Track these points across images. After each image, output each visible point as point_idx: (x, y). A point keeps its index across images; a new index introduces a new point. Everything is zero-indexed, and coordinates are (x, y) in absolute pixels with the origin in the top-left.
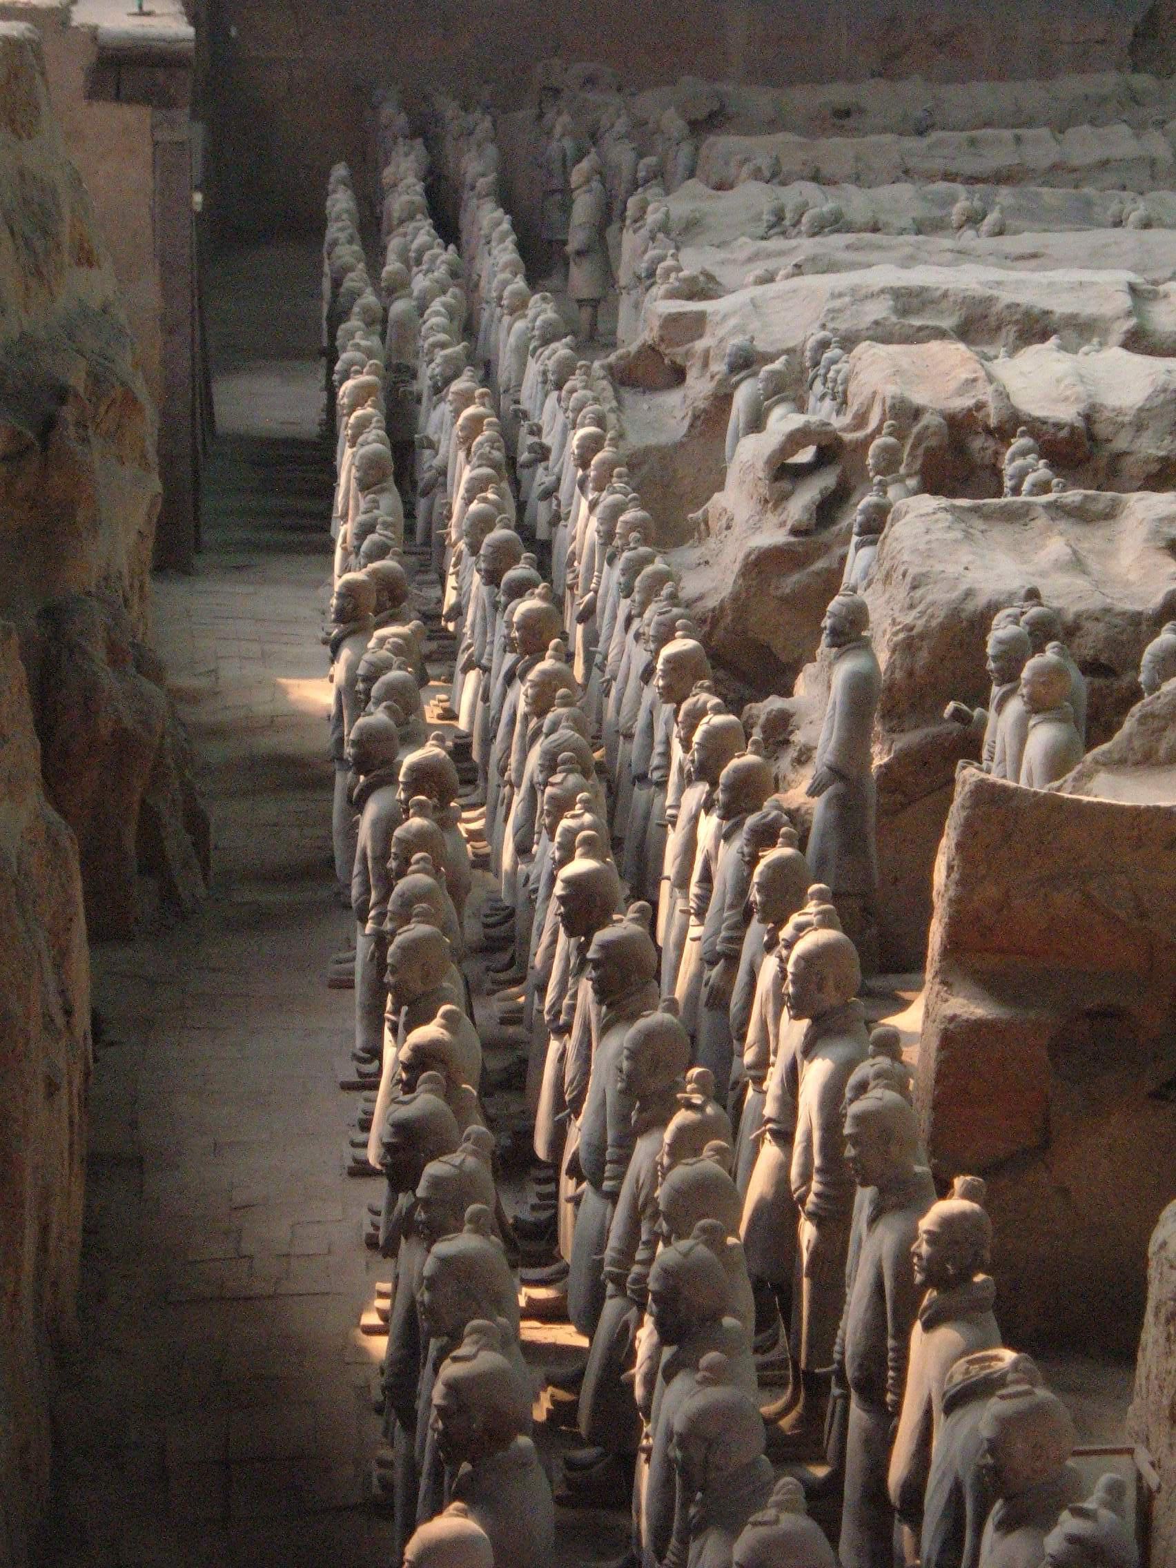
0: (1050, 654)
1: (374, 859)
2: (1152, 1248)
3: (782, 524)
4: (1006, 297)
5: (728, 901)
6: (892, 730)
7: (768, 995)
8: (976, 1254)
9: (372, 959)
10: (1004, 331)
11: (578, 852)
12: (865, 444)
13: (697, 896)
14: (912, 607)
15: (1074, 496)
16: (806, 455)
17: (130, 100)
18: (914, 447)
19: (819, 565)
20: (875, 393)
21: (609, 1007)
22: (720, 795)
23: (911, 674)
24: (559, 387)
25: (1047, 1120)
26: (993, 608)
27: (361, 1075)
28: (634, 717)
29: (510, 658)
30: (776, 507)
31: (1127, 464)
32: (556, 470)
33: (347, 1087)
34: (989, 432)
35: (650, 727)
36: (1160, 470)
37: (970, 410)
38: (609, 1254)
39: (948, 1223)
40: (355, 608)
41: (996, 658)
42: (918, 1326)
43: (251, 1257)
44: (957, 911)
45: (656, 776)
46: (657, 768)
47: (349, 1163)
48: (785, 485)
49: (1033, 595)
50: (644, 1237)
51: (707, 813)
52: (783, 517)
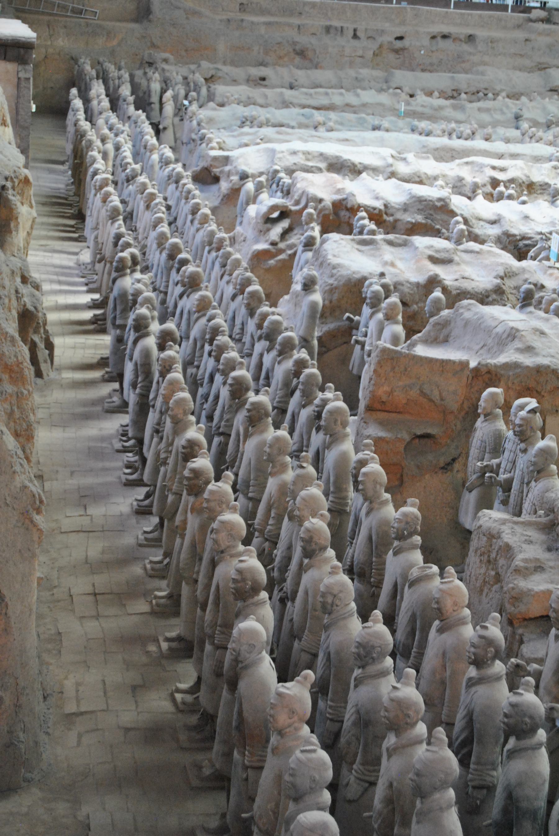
0: (394, 299)
1: (141, 365)
3: (266, 241)
5: (279, 386)
6: (322, 323)
9: (138, 403)
11: (237, 367)
14: (332, 276)
15: (391, 237)
16: (275, 215)
17: (10, 61)
19: (282, 257)
20: (303, 192)
23: (331, 302)
24: (177, 182)
25: (402, 476)
26: (365, 279)
27: (123, 446)
29: (179, 289)
30: (265, 234)
31: (399, 226)
32: (175, 215)
33: (118, 451)
34: (347, 209)
35: (234, 318)
36: (412, 228)
38: (257, 521)
39: (405, 515)
41: (370, 298)
42: (391, 552)
43: (91, 516)
44: (373, 396)
45: (237, 337)
46: (238, 334)
47: (124, 481)
48: (269, 225)
49: (382, 275)
50: (273, 515)
51: (268, 353)
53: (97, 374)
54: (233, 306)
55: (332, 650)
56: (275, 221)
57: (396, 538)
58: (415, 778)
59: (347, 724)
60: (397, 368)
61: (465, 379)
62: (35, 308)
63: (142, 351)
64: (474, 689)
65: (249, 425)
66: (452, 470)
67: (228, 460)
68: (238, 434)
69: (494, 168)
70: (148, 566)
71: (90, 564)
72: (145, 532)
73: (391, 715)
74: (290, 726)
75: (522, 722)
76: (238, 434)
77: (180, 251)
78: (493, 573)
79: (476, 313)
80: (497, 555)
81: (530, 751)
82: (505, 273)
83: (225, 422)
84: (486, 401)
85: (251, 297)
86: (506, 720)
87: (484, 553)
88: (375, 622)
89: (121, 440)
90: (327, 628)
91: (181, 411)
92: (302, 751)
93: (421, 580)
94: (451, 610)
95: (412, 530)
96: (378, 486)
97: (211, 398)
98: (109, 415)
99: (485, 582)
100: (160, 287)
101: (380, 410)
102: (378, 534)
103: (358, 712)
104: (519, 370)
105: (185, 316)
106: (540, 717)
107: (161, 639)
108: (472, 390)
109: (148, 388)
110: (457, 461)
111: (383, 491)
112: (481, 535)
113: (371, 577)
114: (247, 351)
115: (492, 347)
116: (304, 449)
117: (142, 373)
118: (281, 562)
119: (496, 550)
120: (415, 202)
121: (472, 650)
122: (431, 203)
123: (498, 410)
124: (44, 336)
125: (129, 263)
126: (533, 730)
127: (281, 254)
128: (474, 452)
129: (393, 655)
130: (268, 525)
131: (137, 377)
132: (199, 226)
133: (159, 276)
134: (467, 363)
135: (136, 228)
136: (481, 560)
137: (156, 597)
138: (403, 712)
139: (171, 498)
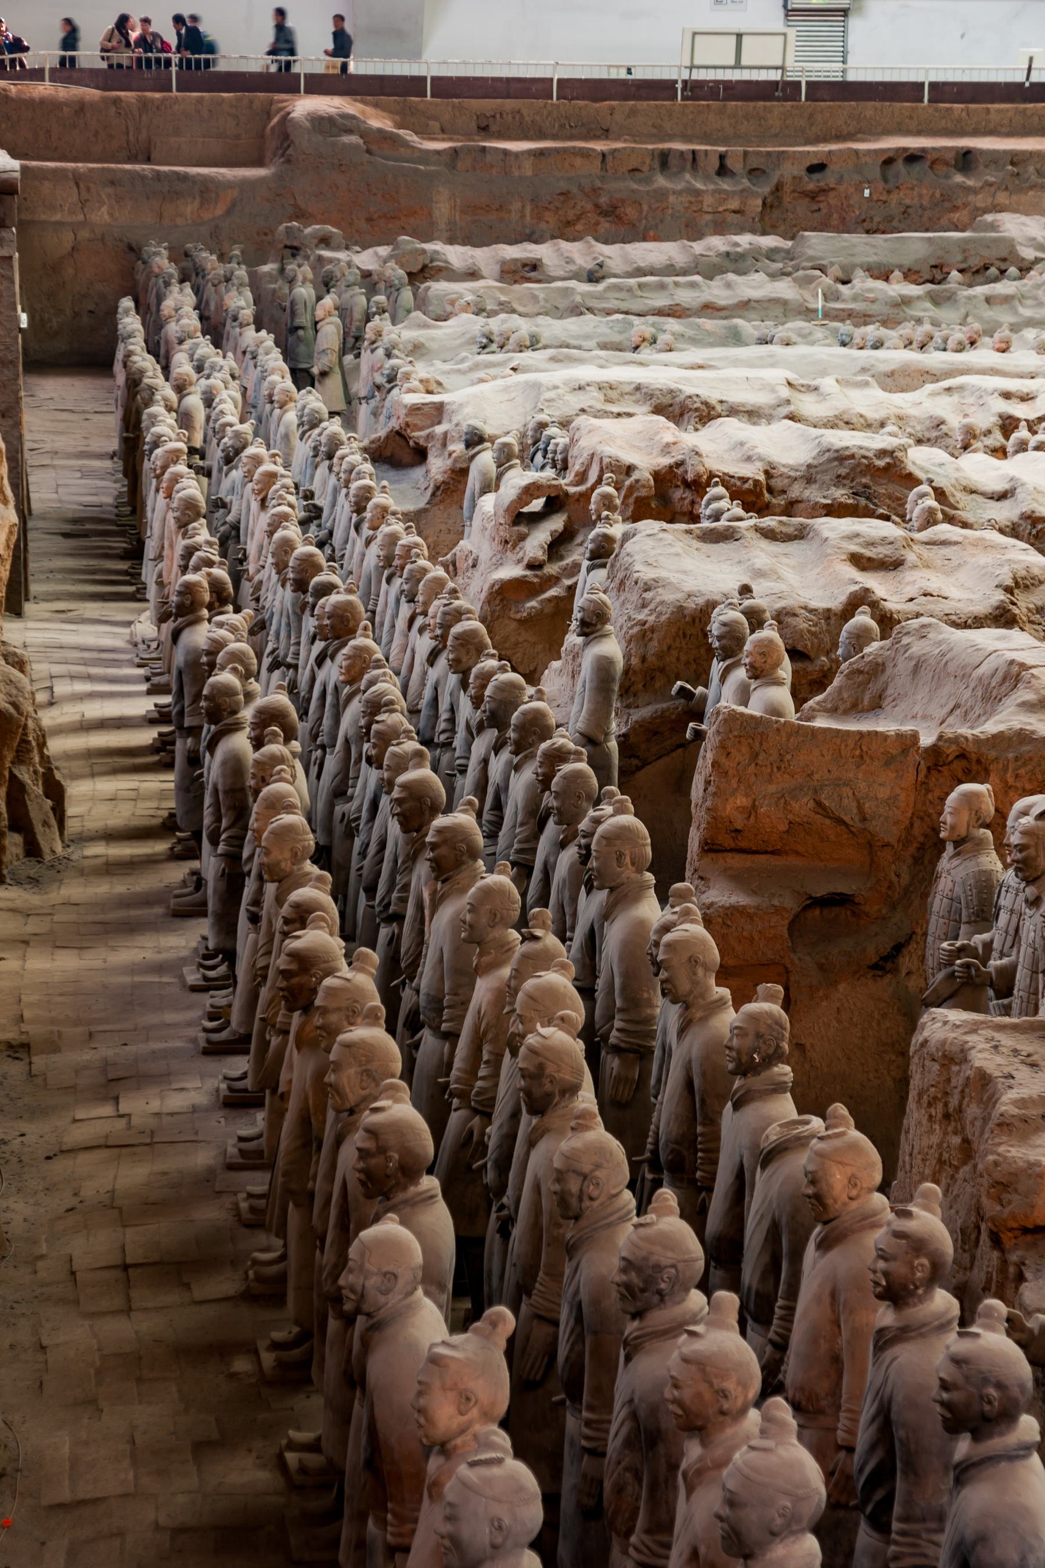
0: (769, 633)
1: (225, 792)
2: (912, 1049)
3: (519, 561)
4: (689, 390)
6: (628, 707)
7: (564, 881)
8: (778, 1047)
9: (223, 875)
10: (686, 417)
12: (586, 496)
13: (489, 822)
15: (769, 522)
16: (537, 505)
18: (626, 497)
20: (593, 455)
21: (443, 882)
22: (511, 734)
23: (644, 659)
24: (330, 456)
26: (712, 605)
27: (205, 978)
28: (420, 696)
30: (514, 547)
32: (328, 525)
33: (194, 989)
34: (687, 485)
35: (435, 701)
37: (671, 467)
40: (192, 603)
43: (129, 1115)
45: (443, 737)
46: (443, 732)
47: (203, 1044)
48: (523, 529)
50: (485, 1057)
52: (521, 554)
53: (161, 847)
54: (433, 674)
55: (584, 1296)
56: (535, 519)
57: (734, 1073)
58: (726, 1511)
59: (613, 1445)
60: (762, 756)
61: (912, 771)
62: (15, 705)
63: (224, 763)
64: (889, 1354)
65: (436, 879)
66: (896, 971)
67: (403, 965)
68: (420, 906)
69: (1007, 395)
70: (244, 1205)
71: (120, 1209)
72: (241, 1139)
73: (687, 1394)
74: (462, 1431)
75: (981, 1397)
76: (420, 906)
77: (318, 569)
78: (956, 1140)
79: (940, 643)
80: (963, 1098)
81: (1003, 1464)
82: (1015, 579)
83: (399, 891)
84: (955, 812)
85: (462, 645)
86: (945, 1396)
87: (935, 1098)
88: (666, 1211)
89: (201, 966)
90: (571, 1249)
91: (287, 854)
92: (473, 1464)
93: (786, 1149)
94: (844, 1198)
95: (771, 1051)
96: (700, 972)
97: (372, 849)
98: (176, 920)
99: (941, 1162)
100: (286, 656)
101: (731, 850)
102: (704, 1074)
103: (634, 1415)
104: (1026, 748)
105: (329, 699)
106: (1022, 1387)
107: (262, 1345)
108: (930, 796)
109: (238, 841)
110: (905, 951)
111: (713, 981)
112: (927, 1063)
113: (697, 1169)
114: (458, 762)
115: (972, 708)
116: (568, 934)
117: (228, 809)
118: (499, 1146)
119: (960, 1089)
120: (830, 460)
121: (881, 1265)
122: (864, 461)
123: (982, 830)
124: (41, 770)
125: (207, 597)
126: (1007, 1416)
127: (550, 587)
128: (935, 924)
129: (705, 1287)
130: (477, 1079)
131: (218, 819)
132: (371, 532)
133: (283, 634)
134: (915, 736)
135: (245, 554)
136: (931, 1116)
137: (256, 1262)
138: (711, 1384)
139: (275, 1041)
